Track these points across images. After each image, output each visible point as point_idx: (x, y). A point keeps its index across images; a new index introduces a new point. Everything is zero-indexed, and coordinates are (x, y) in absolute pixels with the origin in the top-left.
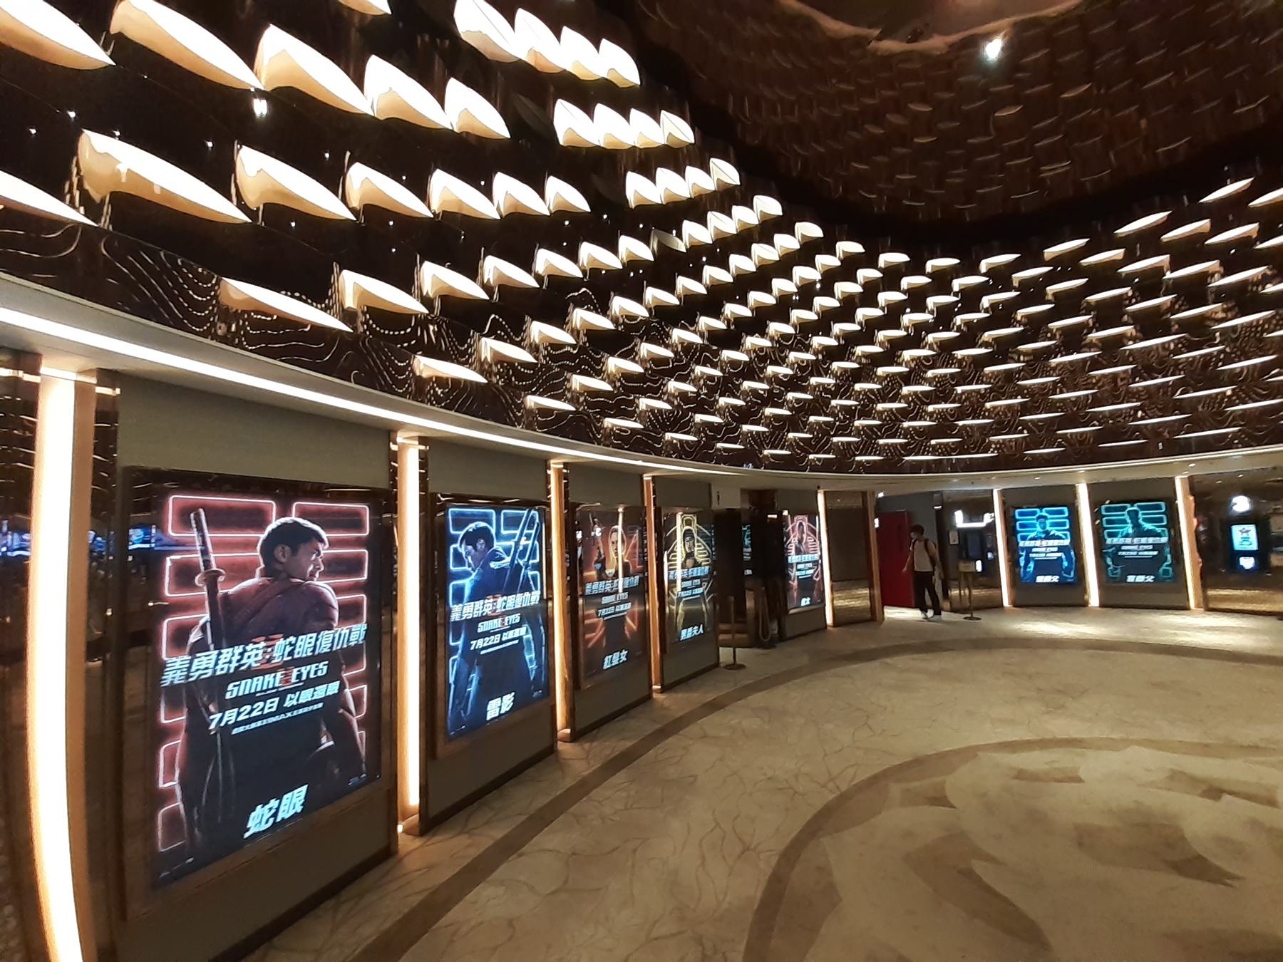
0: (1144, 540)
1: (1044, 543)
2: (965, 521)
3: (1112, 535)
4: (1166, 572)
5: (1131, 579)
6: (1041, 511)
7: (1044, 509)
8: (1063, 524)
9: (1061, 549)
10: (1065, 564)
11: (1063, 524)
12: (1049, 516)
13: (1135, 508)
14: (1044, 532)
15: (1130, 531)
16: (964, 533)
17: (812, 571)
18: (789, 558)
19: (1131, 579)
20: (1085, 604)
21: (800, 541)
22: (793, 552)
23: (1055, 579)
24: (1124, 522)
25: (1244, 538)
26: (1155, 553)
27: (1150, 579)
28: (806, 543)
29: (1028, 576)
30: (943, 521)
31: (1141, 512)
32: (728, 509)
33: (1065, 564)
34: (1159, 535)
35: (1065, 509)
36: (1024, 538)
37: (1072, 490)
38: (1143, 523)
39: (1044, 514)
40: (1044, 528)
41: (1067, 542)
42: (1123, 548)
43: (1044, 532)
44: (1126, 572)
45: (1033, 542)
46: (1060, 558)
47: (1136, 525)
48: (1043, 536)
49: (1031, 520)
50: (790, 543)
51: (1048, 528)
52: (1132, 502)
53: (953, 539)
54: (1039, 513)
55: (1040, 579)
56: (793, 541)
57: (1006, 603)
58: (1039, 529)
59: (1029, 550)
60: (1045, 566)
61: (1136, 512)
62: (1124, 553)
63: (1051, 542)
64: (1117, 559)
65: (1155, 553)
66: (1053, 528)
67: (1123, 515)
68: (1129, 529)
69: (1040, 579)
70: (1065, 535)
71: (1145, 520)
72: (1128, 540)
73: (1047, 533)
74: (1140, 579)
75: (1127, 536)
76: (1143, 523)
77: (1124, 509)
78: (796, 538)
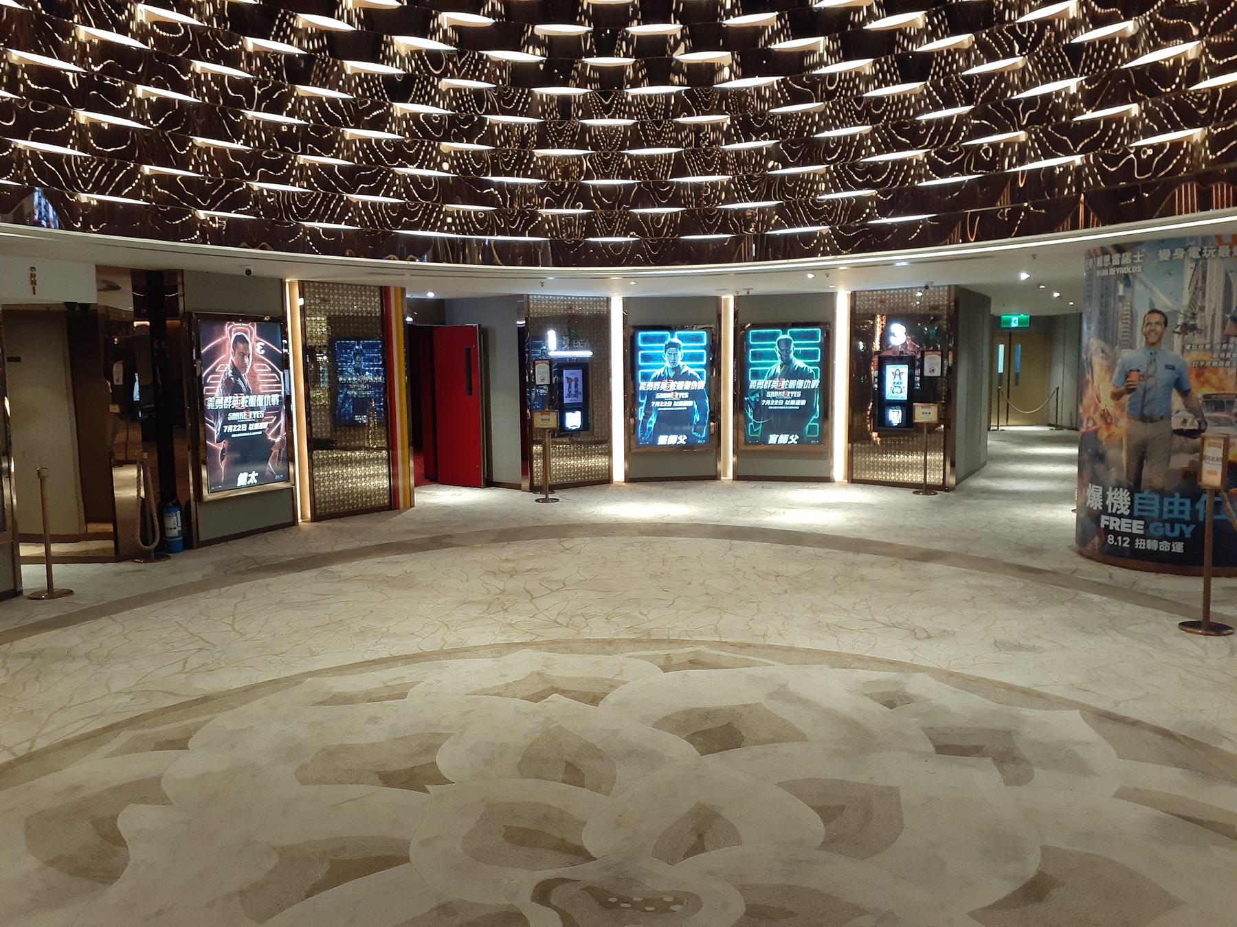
0: (792, 384)
1: (673, 385)
2: (560, 347)
3: (756, 375)
4: (812, 429)
5: (773, 439)
6: (672, 337)
7: (677, 333)
8: (699, 357)
9: (693, 395)
10: (697, 418)
11: (699, 357)
12: (682, 345)
13: (788, 336)
14: (674, 369)
15: (779, 371)
16: (559, 366)
17: (264, 425)
18: (210, 400)
19: (773, 439)
20: (715, 477)
21: (236, 372)
22: (219, 389)
23: (682, 440)
24: (773, 356)
25: (896, 382)
26: (803, 402)
27: (794, 439)
28: (253, 375)
29: (648, 434)
30: (527, 342)
31: (793, 342)
32: (67, 304)
33: (697, 418)
34: (810, 377)
35: (704, 334)
36: (646, 377)
37: (715, 303)
38: (794, 359)
39: (675, 340)
40: (674, 362)
41: (701, 385)
42: (769, 394)
43: (674, 369)
44: (769, 430)
45: (657, 384)
46: (690, 408)
47: (787, 362)
48: (672, 374)
49: (656, 349)
50: (213, 372)
51: (680, 363)
52: (784, 326)
53: (542, 374)
54: (669, 340)
55: (663, 440)
56: (224, 366)
57: (619, 475)
58: (667, 364)
59: (651, 395)
60: (671, 420)
61: (788, 342)
62: (768, 402)
63: (681, 385)
64: (760, 411)
65: (803, 402)
66: (684, 363)
67: (773, 346)
68: (777, 367)
69: (663, 440)
70: (700, 374)
71: (796, 354)
72: (775, 383)
73: (677, 369)
74: (783, 439)
75: (773, 377)
76: (794, 359)
77: (773, 337)
78: (228, 366)
